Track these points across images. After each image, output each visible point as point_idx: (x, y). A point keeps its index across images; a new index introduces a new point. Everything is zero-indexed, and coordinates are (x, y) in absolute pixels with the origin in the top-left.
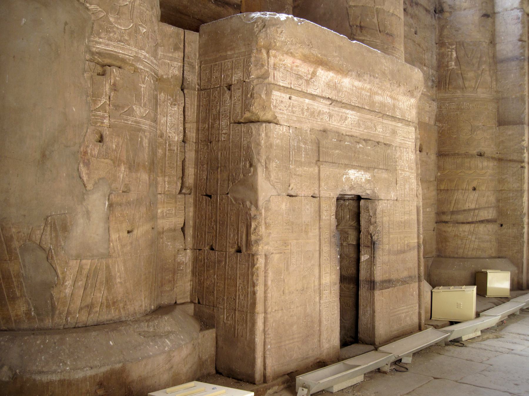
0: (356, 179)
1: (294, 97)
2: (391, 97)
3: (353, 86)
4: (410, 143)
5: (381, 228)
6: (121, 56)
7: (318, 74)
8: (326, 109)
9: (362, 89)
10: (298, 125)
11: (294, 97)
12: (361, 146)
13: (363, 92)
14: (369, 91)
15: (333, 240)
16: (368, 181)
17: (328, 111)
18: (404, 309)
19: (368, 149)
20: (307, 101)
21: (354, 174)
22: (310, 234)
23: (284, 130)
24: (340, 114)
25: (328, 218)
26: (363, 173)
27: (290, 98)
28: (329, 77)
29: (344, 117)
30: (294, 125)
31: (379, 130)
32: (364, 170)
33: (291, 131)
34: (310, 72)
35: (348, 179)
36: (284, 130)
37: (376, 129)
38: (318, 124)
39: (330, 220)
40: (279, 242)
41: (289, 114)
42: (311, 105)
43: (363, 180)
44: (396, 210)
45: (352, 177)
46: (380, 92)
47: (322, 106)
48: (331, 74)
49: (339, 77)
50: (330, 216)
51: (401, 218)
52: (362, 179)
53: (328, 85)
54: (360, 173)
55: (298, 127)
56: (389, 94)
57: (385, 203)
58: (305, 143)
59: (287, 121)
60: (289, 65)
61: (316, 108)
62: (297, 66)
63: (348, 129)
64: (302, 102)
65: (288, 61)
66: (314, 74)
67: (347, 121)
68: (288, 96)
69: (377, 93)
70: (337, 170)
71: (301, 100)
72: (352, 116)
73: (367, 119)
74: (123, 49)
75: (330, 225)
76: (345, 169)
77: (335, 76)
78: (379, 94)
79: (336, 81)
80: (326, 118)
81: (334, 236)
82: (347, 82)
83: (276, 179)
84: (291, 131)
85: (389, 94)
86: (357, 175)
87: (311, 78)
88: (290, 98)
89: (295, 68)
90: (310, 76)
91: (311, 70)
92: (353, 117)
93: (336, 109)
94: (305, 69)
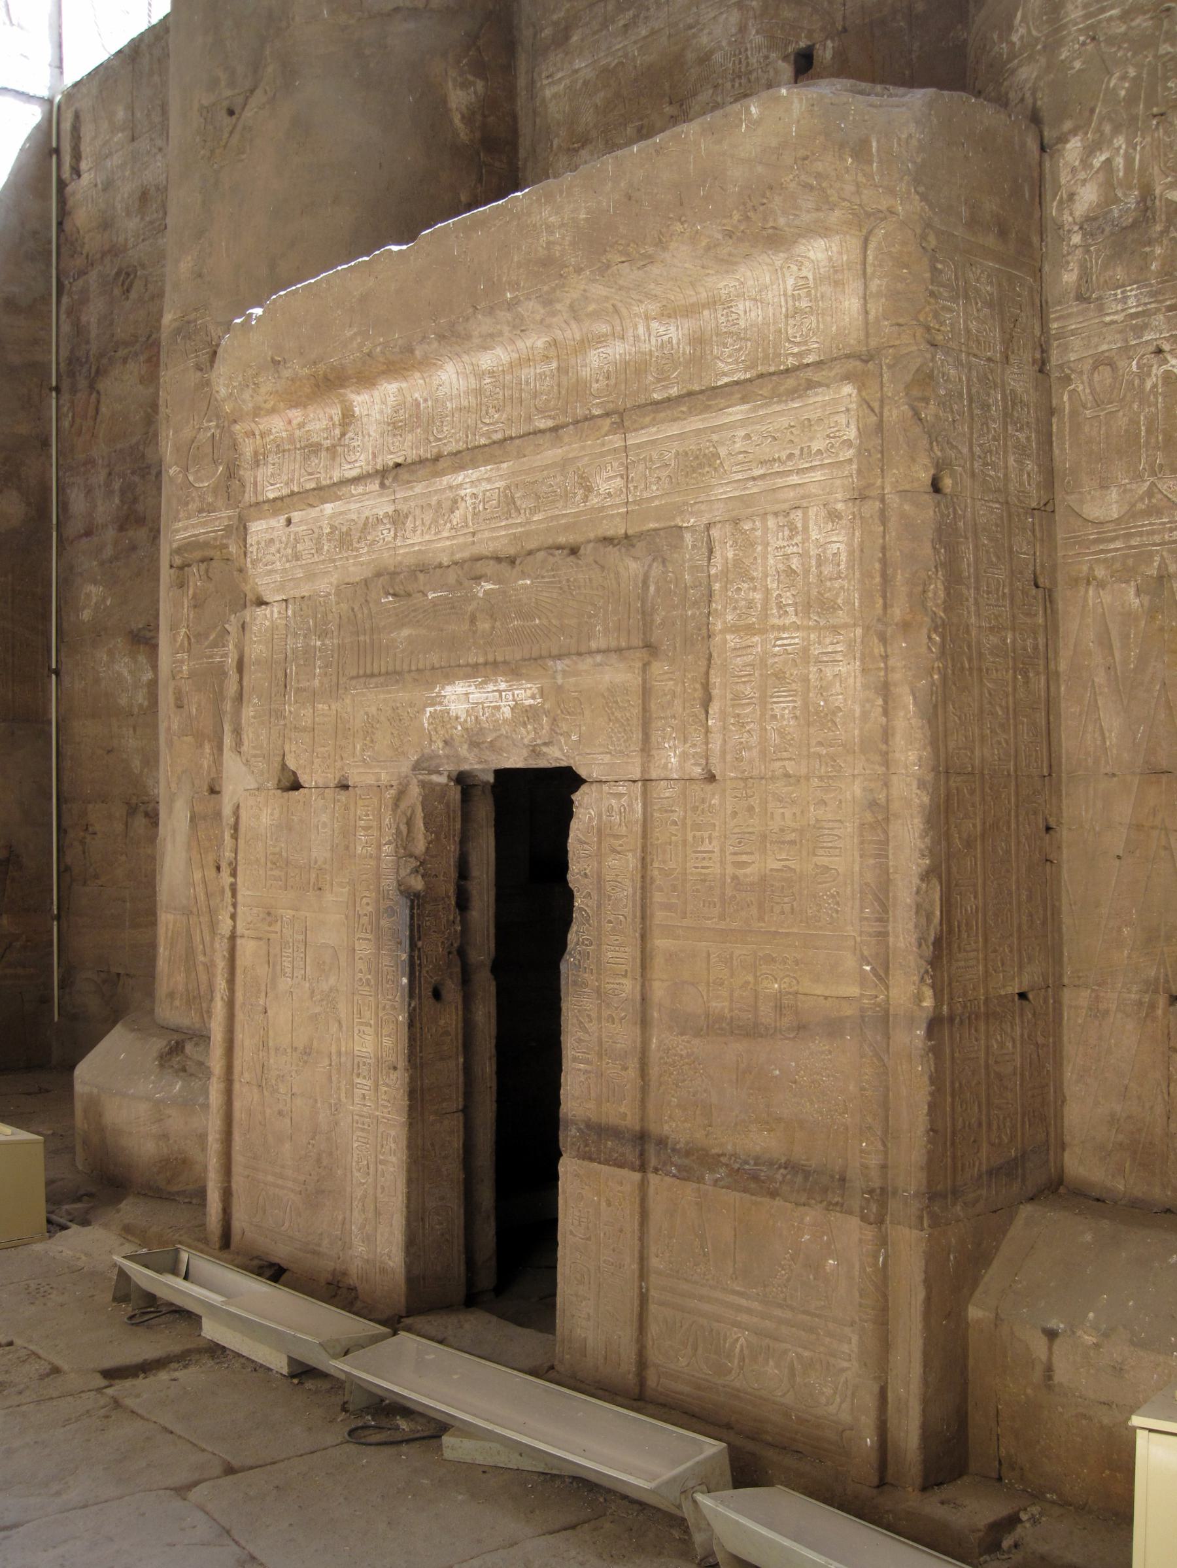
0: (485, 713)
1: (296, 516)
2: (670, 313)
3: (480, 375)
4: (818, 476)
5: (593, 903)
6: (202, 538)
7: (357, 413)
8: (383, 507)
9: (522, 362)
10: (305, 590)
11: (296, 516)
12: (489, 586)
13: (526, 373)
14: (552, 352)
15: (385, 923)
16: (525, 715)
17: (390, 509)
18: (749, 1311)
19: (525, 587)
20: (329, 508)
21: (461, 698)
22: (329, 897)
23: (276, 615)
24: (434, 500)
25: (372, 850)
26: (503, 686)
27: (289, 522)
28: (391, 400)
29: (447, 505)
30: (297, 593)
31: (604, 487)
32: (504, 674)
33: (290, 612)
34: (336, 419)
35: (443, 719)
36: (276, 615)
37: (589, 489)
38: (357, 564)
39: (378, 858)
40: (255, 910)
41: (287, 565)
42: (342, 513)
43: (507, 712)
44: (697, 827)
45: (457, 708)
46: (604, 328)
47: (371, 503)
48: (390, 390)
49: (417, 379)
50: (379, 847)
51: (743, 865)
52: (498, 708)
53: (395, 427)
54: (491, 687)
55: (306, 594)
56: (653, 307)
57: (621, 795)
58: (323, 634)
59: (281, 587)
60: (284, 434)
61: (354, 517)
62: (301, 426)
63: (461, 540)
64: (316, 519)
65: (276, 425)
66: (348, 417)
67: (457, 517)
68: (282, 519)
69: (586, 344)
70: (403, 695)
71: (313, 513)
72: (474, 484)
73: (547, 467)
74: (204, 524)
75: (378, 877)
76: (430, 685)
77: (404, 385)
78: (601, 340)
79: (417, 395)
80: (386, 533)
81: (391, 911)
82: (450, 378)
83: (254, 748)
84: (290, 612)
85: (653, 307)
86: (477, 696)
87: (343, 434)
88: (289, 522)
89: (297, 433)
90: (337, 432)
91: (336, 412)
92: (485, 486)
93: (419, 488)
94: (319, 420)
